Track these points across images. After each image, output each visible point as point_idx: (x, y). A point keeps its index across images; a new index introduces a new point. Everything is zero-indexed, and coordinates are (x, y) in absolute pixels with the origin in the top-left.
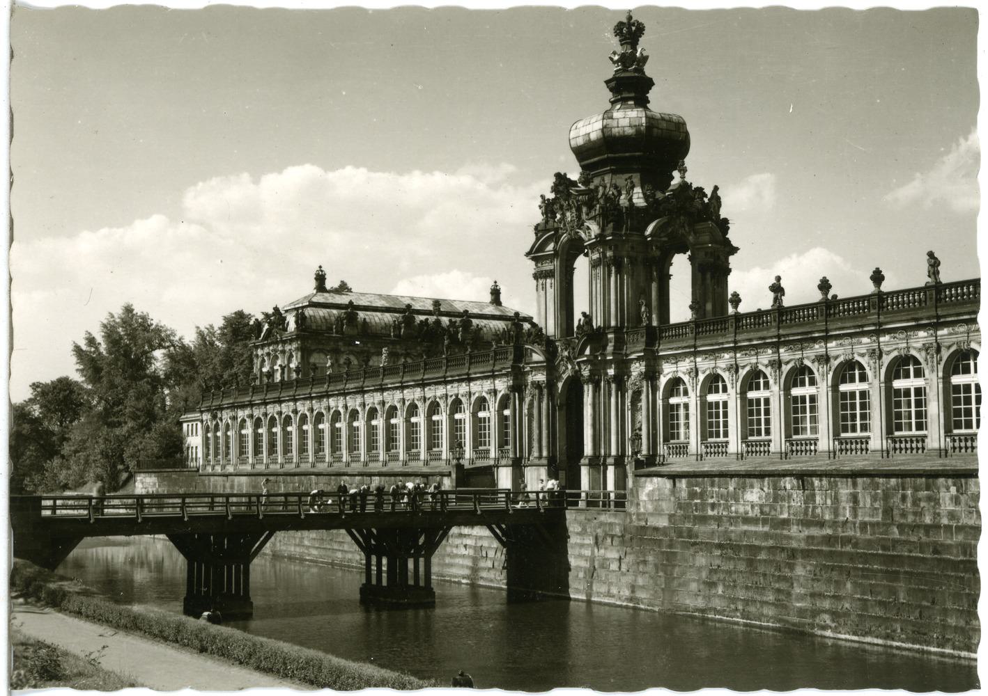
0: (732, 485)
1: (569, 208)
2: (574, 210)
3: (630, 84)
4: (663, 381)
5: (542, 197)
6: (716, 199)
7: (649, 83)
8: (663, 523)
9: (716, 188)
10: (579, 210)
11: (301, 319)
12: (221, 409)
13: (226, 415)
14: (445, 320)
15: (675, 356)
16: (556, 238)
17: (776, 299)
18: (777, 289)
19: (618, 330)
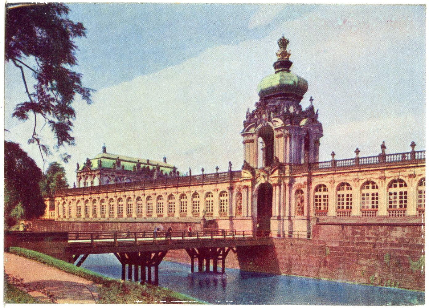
0: (382, 230)
1: (265, 113)
2: (267, 114)
3: (284, 64)
4: (314, 186)
10: (269, 114)
14: (151, 167)
15: (321, 175)
19: (290, 164)
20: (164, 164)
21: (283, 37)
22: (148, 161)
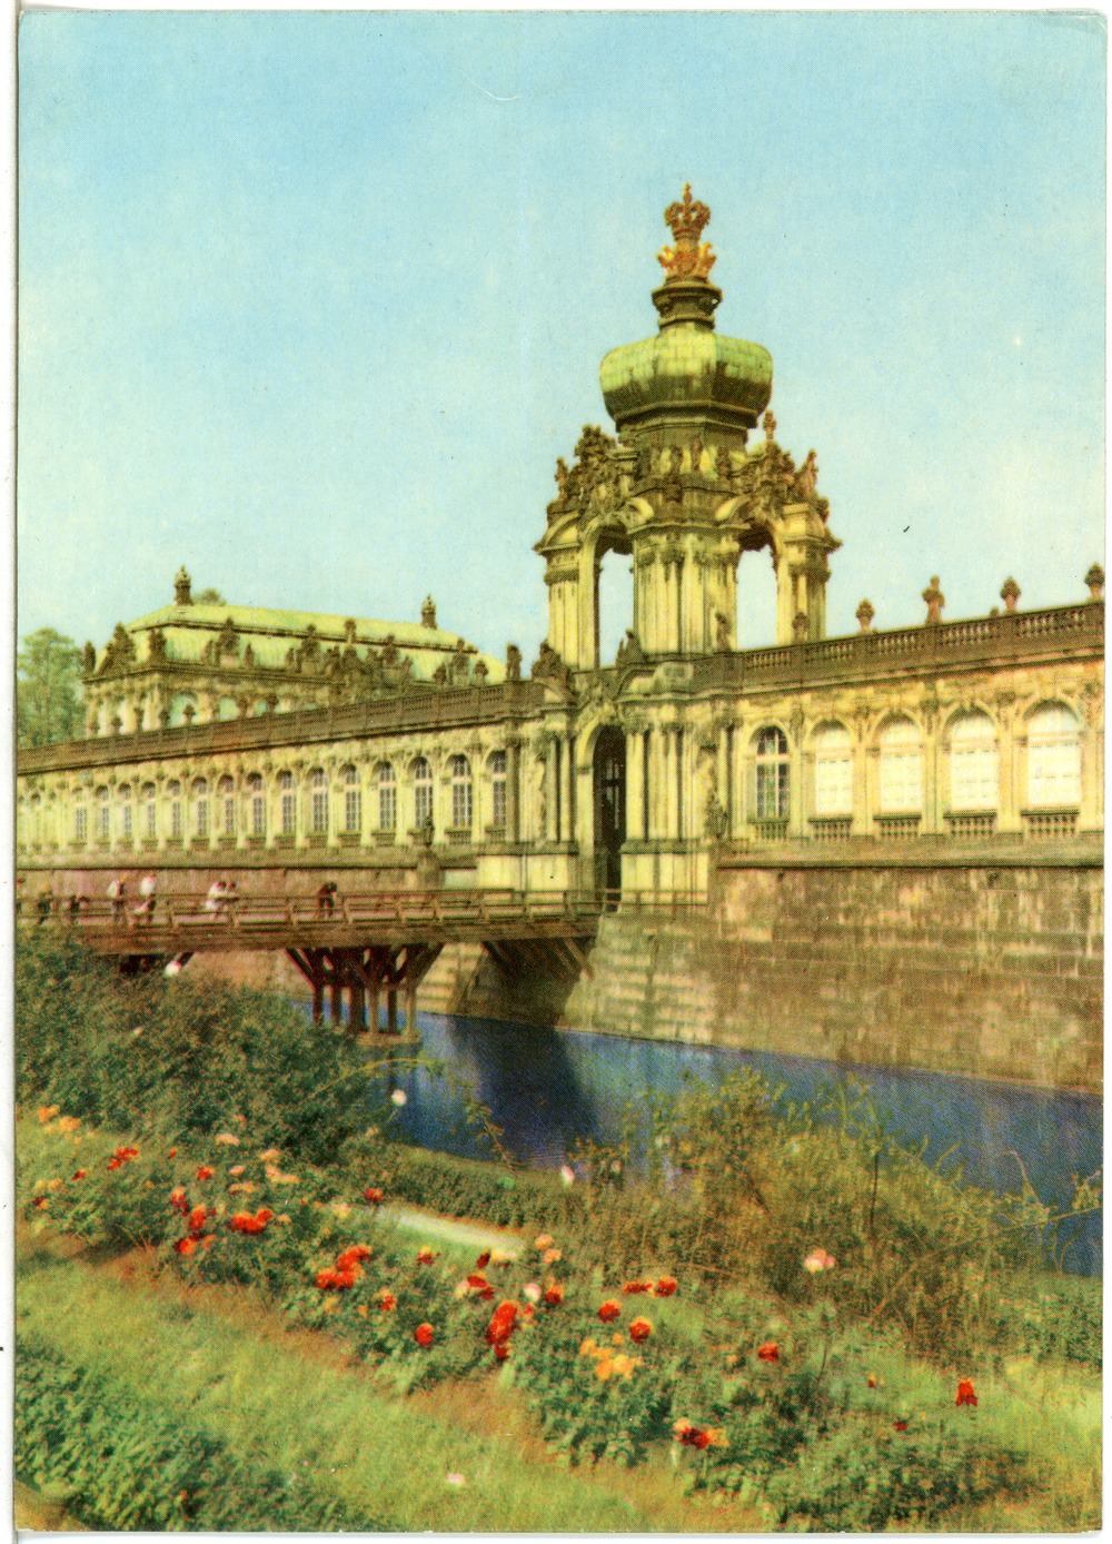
0: (878, 882)
3: (689, 300)
5: (560, 462)
6: (810, 468)
8: (761, 936)
9: (811, 456)
10: (617, 482)
11: (158, 644)
12: (41, 772)
14: (362, 652)
17: (932, 613)
18: (933, 597)
20: (424, 635)
21: (688, 197)
22: (350, 625)
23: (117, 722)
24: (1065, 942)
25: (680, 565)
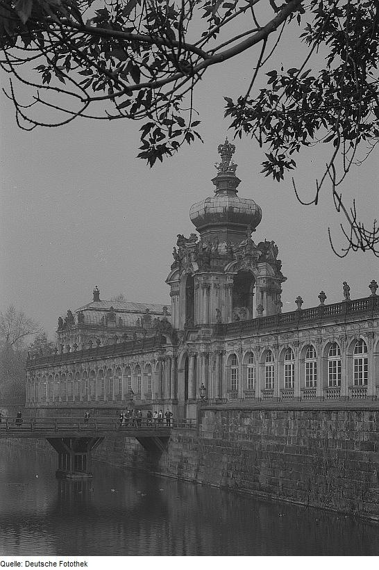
3: (227, 182)
7: (238, 181)
10: (189, 256)
11: (81, 317)
13: (37, 373)
16: (180, 271)
21: (227, 142)
22: (165, 308)
23: (69, 348)
24: (281, 439)
25: (209, 289)
